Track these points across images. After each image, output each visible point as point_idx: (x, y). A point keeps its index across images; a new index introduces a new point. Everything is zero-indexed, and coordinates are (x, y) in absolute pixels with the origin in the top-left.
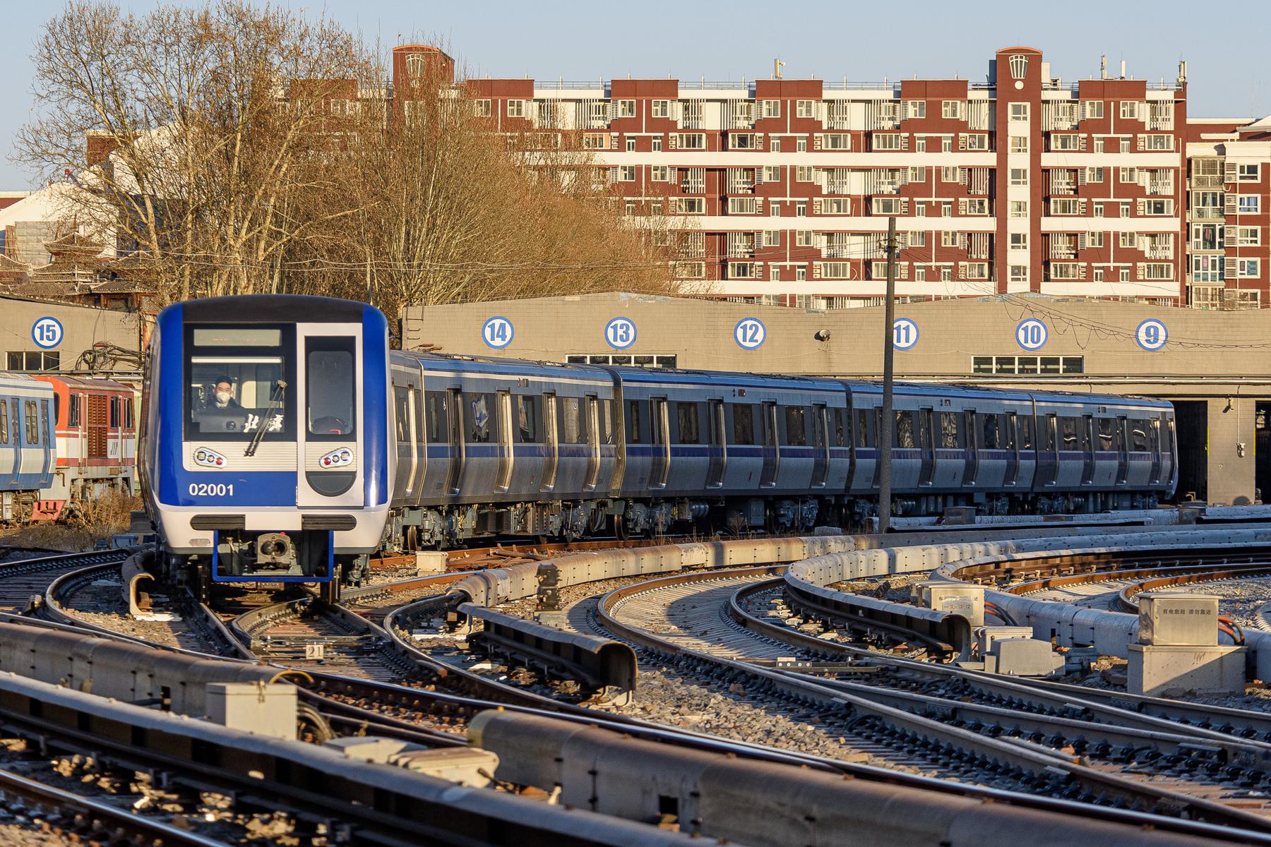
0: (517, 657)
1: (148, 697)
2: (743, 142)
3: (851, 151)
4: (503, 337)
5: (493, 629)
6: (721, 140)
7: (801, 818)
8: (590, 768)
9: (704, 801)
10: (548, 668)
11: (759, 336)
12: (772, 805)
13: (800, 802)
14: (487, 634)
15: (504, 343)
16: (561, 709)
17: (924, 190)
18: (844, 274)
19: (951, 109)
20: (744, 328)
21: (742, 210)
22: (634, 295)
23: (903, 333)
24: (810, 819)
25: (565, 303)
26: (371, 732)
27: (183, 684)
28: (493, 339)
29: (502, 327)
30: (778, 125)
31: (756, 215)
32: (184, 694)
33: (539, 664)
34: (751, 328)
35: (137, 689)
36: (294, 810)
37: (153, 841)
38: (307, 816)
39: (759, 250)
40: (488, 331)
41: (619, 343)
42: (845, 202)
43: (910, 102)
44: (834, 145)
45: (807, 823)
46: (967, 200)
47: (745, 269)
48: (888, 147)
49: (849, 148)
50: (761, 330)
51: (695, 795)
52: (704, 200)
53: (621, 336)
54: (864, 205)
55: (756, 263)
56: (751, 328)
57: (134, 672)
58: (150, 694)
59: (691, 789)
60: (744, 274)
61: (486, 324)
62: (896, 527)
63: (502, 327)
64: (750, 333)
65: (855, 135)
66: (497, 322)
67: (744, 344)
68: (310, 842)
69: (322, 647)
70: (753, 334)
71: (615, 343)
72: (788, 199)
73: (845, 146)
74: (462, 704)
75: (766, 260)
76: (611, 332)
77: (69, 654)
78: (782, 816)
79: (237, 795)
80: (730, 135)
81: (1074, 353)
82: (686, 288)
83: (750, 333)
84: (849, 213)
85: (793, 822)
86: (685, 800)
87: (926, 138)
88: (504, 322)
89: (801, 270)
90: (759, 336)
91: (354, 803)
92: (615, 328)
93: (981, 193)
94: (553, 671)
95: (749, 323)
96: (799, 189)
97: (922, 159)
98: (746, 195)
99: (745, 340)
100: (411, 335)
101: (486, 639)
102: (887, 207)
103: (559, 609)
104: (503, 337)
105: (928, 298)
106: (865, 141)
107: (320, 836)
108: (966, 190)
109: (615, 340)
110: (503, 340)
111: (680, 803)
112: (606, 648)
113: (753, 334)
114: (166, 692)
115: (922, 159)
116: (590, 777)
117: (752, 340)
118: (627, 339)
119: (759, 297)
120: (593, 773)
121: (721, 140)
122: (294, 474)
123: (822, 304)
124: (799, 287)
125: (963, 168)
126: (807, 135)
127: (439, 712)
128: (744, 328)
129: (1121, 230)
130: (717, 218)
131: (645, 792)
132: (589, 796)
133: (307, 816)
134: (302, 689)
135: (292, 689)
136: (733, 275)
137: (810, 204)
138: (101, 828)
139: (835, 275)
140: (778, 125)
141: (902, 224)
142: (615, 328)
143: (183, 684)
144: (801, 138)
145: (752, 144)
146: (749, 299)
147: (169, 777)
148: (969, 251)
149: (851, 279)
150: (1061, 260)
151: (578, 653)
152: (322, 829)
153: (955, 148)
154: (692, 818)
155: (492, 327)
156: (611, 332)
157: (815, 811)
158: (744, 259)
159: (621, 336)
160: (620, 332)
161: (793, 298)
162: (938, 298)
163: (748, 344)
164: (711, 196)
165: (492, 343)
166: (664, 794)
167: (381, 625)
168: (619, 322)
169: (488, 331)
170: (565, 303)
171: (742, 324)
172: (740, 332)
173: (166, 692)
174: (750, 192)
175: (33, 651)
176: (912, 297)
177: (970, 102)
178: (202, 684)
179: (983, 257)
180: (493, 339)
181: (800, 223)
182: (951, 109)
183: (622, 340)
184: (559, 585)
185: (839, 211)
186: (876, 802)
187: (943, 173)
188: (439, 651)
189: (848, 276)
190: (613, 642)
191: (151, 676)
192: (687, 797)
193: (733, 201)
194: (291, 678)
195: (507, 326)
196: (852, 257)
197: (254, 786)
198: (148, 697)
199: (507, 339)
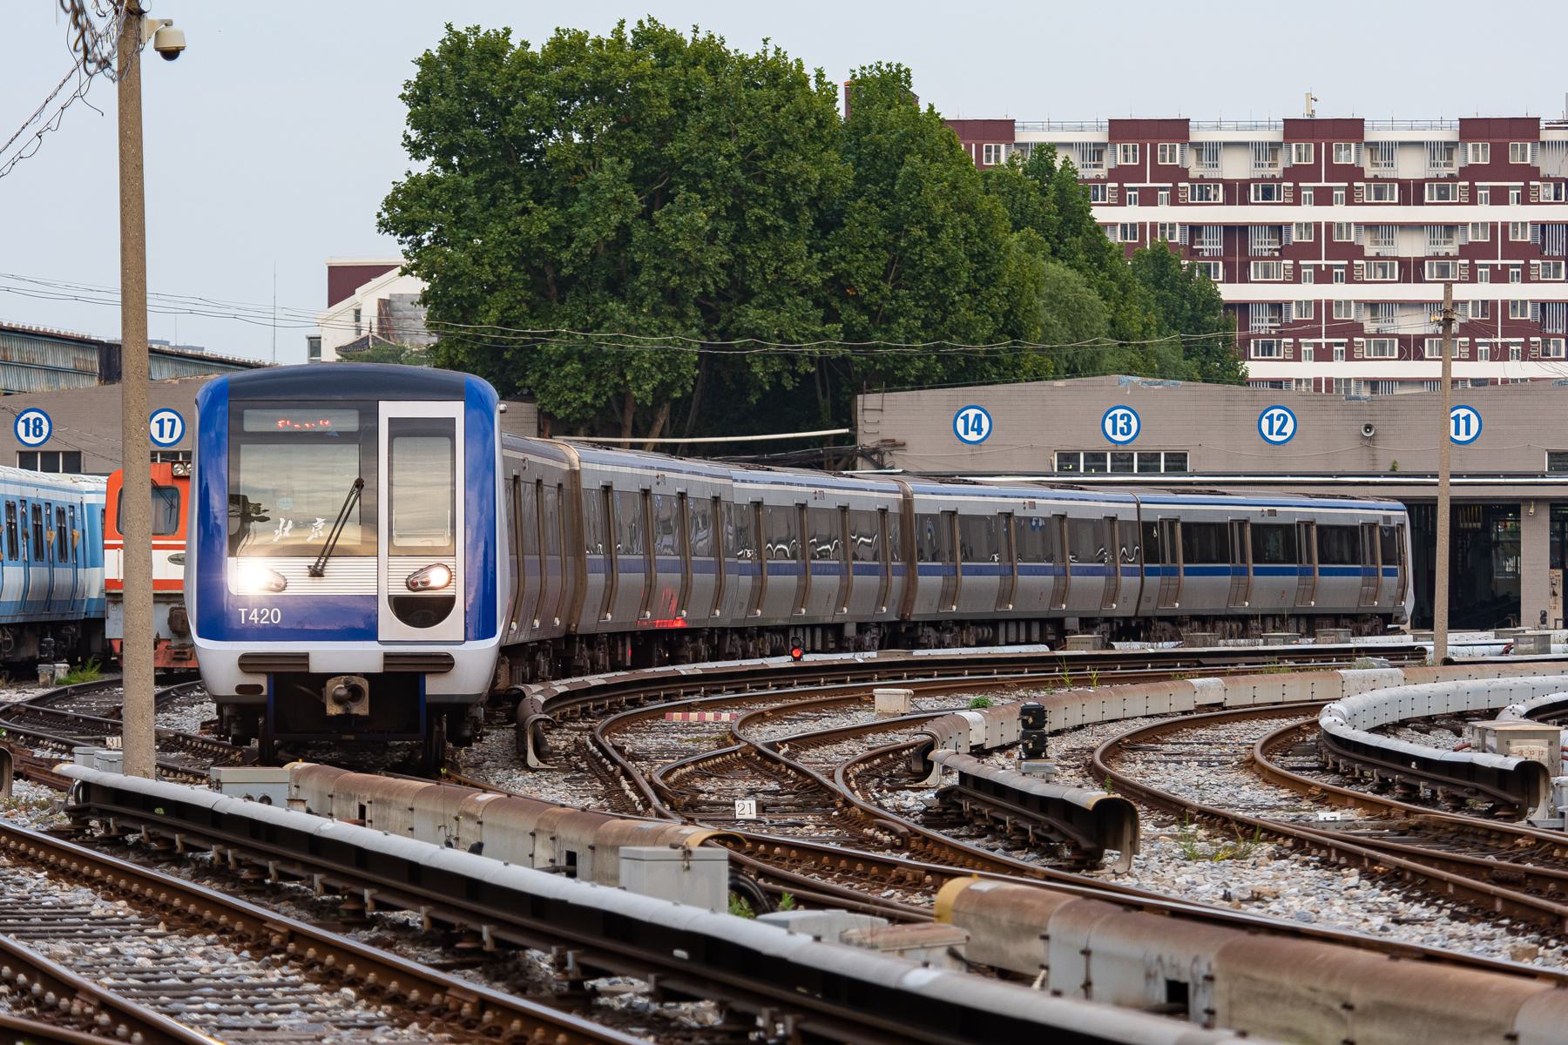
0: (997, 815)
1: (550, 865)
2: (1268, 194)
3: (1399, 204)
4: (979, 431)
5: (970, 783)
6: (1236, 192)
7: (1337, 1006)
8: (1083, 947)
9: (1220, 985)
10: (1033, 828)
11: (1289, 428)
12: (1304, 992)
13: (1335, 986)
14: (963, 789)
15: (980, 437)
16: (1049, 878)
17: (1487, 250)
18: (1392, 353)
19: (1522, 154)
20: (1271, 418)
21: (1267, 275)
22: (1136, 379)
23: (1463, 423)
24: (1348, 1007)
25: (1055, 389)
26: (799, 902)
27: (592, 848)
28: (966, 433)
29: (978, 417)
30: (1311, 173)
31: (1284, 282)
32: (593, 861)
33: (1023, 825)
34: (1278, 419)
35: (536, 855)
36: (726, 998)
37: (556, 1036)
38: (740, 1006)
39: (1288, 325)
40: (960, 424)
41: (1119, 437)
42: (1392, 266)
43: (1470, 145)
44: (1379, 196)
45: (1344, 1012)
46: (1538, 262)
47: (1270, 346)
48: (1444, 197)
49: (1396, 200)
50: (1290, 421)
51: (1210, 978)
52: (1221, 263)
53: (1122, 429)
54: (1411, 270)
55: (1284, 340)
56: (1278, 419)
57: (533, 834)
58: (552, 861)
59: (1204, 971)
60: (1270, 354)
61: (18, 418)
62: (1455, 659)
63: (978, 417)
64: (1277, 425)
65: (1404, 184)
66: (972, 413)
67: (1270, 437)
68: (746, 1036)
69: (753, 803)
70: (1466, 425)
71: (1114, 437)
72: (1323, 262)
73: (1392, 198)
74: (929, 871)
75: (1296, 336)
76: (1109, 424)
77: (455, 814)
78: (1314, 1004)
79: (658, 980)
80: (1252, 186)
81: (1176, 446)
82: (1256, 369)
83: (1277, 425)
84: (1396, 279)
85: (1328, 1012)
86: (1197, 986)
87: (1492, 188)
88: (979, 412)
89: (1339, 348)
90: (1289, 428)
91: (800, 989)
92: (1114, 418)
93: (1556, 253)
94: (1039, 831)
95: (1276, 412)
96: (1336, 250)
97: (1485, 213)
98: (1272, 258)
99: (1271, 433)
100: (868, 429)
101: (961, 795)
102: (1444, 271)
103: (1046, 757)
104: (979, 431)
105: (1494, 382)
106: (1412, 193)
107: (758, 1029)
108: (1536, 250)
109: (1115, 433)
110: (979, 434)
111: (1191, 989)
112: (1101, 804)
113: (1466, 425)
114: (572, 858)
115: (1485, 213)
116: (1082, 958)
117: (1279, 433)
118: (1129, 432)
119: (1289, 380)
120: (1086, 953)
121: (1236, 192)
122: (376, 598)
123: (1366, 392)
124: (1338, 369)
125: (1534, 224)
126: (1522, 184)
127: (899, 882)
128: (1271, 418)
129: (1335, 297)
130: (1412, 285)
131: (1149, 976)
132: (1082, 981)
133: (740, 1006)
134: (735, 854)
135: (723, 852)
136: (1256, 354)
137: (1350, 269)
138: (493, 1021)
139: (1381, 352)
140: (1311, 173)
141: (1461, 292)
142: (1114, 418)
143: (592, 848)
144: (1339, 188)
145: (1279, 198)
146: (1276, 384)
147: (576, 958)
148: (1542, 324)
149: (1399, 359)
150: (1260, 336)
151: (1065, 809)
152: (760, 1022)
153: (1525, 199)
154: (1205, 1006)
155: (966, 418)
156: (1109, 424)
157: (1357, 996)
158: (1270, 335)
159: (1122, 429)
160: (1120, 423)
161: (1329, 381)
162: (1505, 381)
163: (1275, 438)
164: (1230, 259)
165: (965, 437)
166: (1173, 976)
167: (832, 777)
168: (1119, 412)
169: (960, 424)
170: (1055, 389)
171: (1268, 414)
172: (1265, 423)
173: (572, 858)
174: (1277, 254)
175: (411, 809)
176: (1473, 380)
177: (1543, 143)
178: (615, 849)
179: (1560, 331)
180: (966, 433)
181: (1337, 291)
182: (1522, 154)
183: (1122, 433)
184: (1047, 729)
185: (1385, 276)
186: (1428, 986)
187: (1335, 231)
188: (899, 811)
189: (1396, 356)
190: (1118, 796)
191: (553, 839)
192: (1200, 981)
193: (1256, 266)
194: (723, 839)
195: (984, 416)
196: (1401, 332)
197: (676, 971)
198: (550, 865)
199: (984, 433)
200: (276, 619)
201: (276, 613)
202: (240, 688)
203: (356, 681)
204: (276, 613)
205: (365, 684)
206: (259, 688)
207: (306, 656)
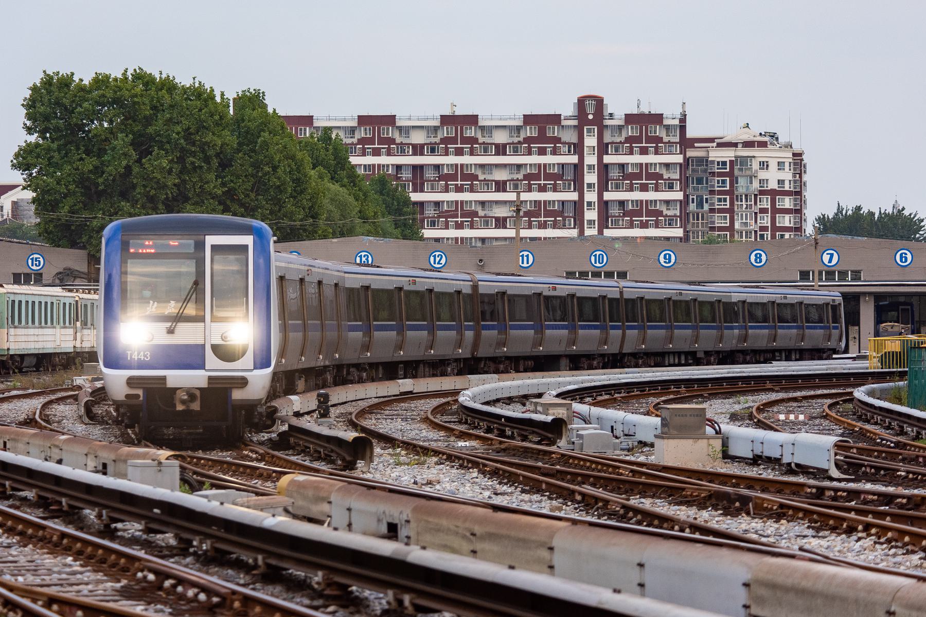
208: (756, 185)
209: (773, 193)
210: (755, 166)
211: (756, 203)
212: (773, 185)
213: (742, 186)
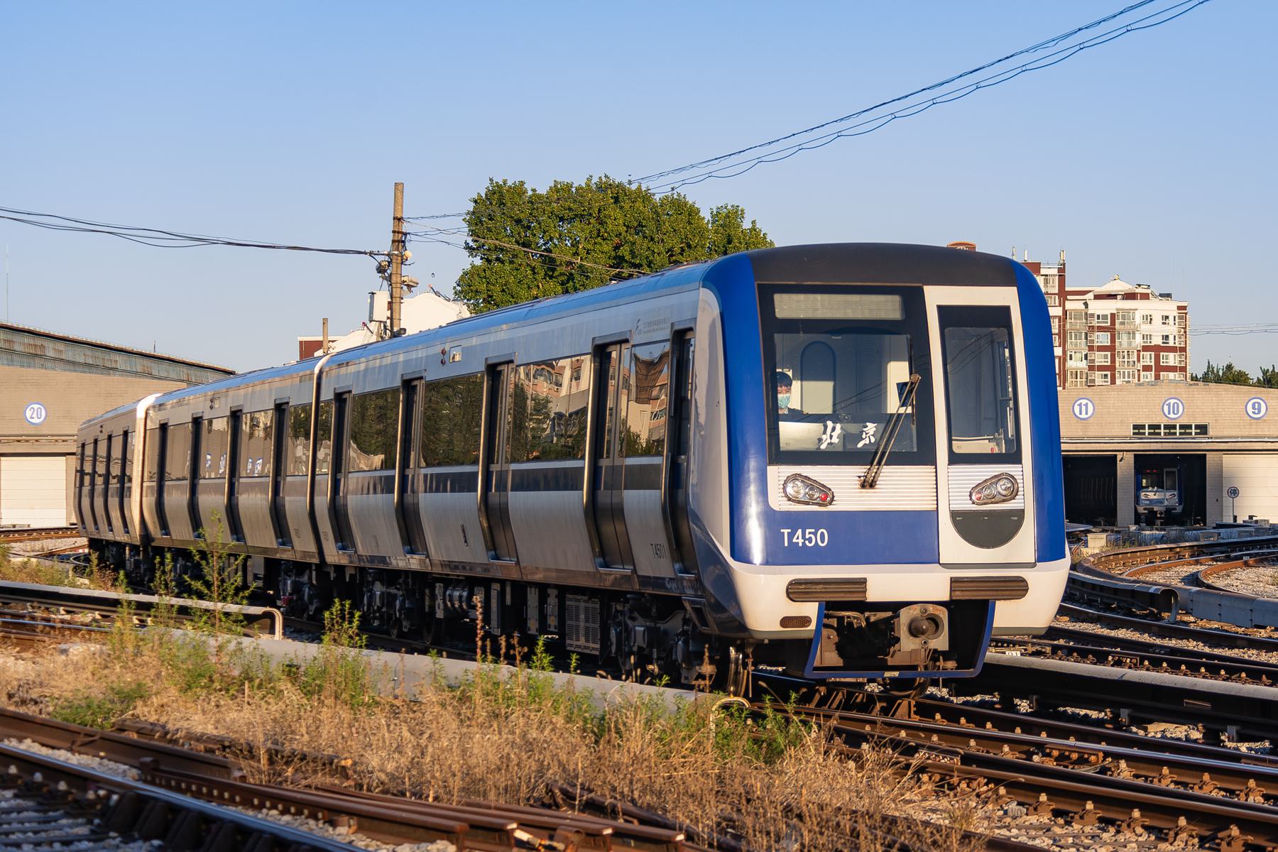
200: (823, 541)
201: (822, 534)
202: (786, 622)
203: (931, 609)
204: (822, 534)
205: (943, 614)
206: (804, 621)
207: (863, 582)
208: (1139, 341)
209: (1157, 349)
210: (1138, 319)
211: (1139, 361)
212: (1157, 341)
213: (1123, 342)
